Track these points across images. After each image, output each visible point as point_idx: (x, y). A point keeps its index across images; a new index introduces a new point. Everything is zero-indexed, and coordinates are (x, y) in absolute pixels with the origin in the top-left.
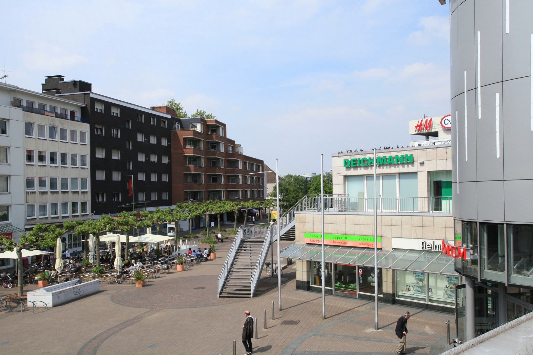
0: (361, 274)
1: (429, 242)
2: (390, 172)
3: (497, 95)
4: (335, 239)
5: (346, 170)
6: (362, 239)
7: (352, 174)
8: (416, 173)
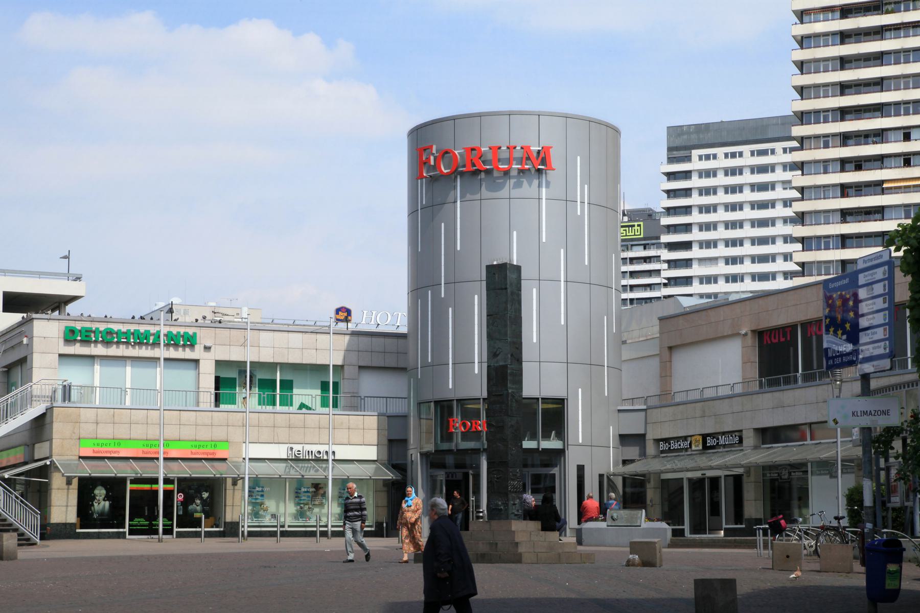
0: (181, 502)
1: (297, 447)
2: (152, 356)
3: (534, 290)
4: (144, 448)
5: (64, 345)
6: (198, 446)
7: (77, 353)
8: (196, 362)
